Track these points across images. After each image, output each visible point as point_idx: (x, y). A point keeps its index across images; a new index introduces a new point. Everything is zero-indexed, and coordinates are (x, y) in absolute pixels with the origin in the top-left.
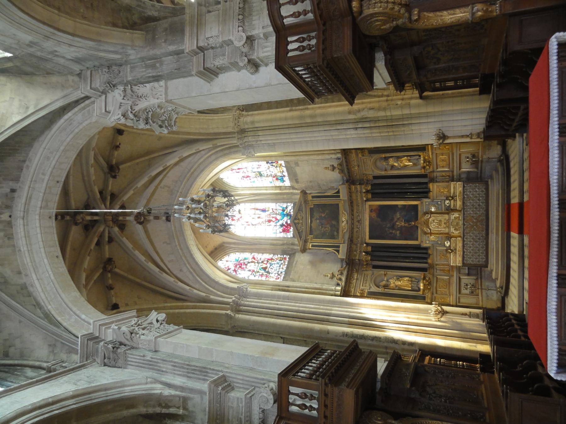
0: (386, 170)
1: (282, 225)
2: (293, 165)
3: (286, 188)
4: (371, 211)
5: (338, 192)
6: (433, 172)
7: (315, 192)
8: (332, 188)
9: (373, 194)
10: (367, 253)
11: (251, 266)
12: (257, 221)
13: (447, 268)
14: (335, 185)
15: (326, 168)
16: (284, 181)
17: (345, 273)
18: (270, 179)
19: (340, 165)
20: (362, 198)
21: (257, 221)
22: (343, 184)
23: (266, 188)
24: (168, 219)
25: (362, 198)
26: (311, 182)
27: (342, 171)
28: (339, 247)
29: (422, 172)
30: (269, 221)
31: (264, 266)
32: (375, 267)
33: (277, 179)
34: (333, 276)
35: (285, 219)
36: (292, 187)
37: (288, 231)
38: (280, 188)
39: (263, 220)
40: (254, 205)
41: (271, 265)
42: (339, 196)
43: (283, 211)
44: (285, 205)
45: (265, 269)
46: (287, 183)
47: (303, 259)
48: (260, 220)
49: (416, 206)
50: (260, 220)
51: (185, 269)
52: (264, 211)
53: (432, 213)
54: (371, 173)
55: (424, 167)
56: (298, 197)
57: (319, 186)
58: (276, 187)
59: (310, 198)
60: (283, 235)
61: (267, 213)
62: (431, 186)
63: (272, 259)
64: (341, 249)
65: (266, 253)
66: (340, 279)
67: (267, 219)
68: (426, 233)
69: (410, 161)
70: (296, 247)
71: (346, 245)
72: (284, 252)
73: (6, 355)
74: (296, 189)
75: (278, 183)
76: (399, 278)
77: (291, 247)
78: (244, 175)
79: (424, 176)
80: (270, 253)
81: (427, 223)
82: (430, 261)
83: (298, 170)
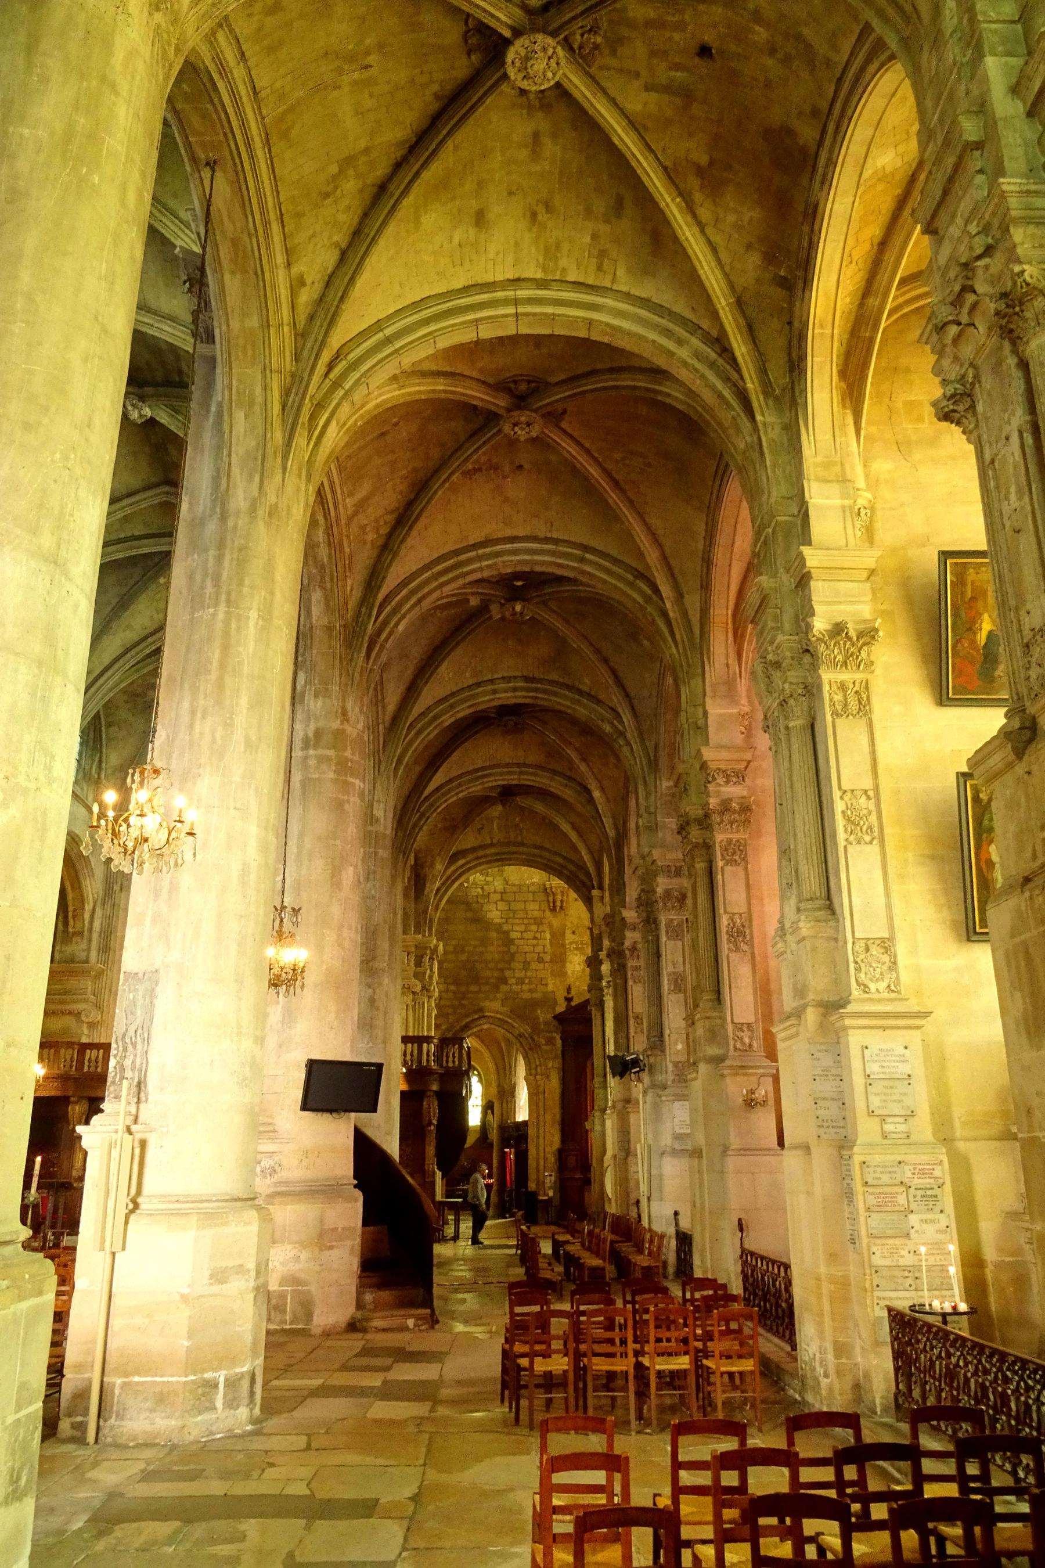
73: (109, 725)
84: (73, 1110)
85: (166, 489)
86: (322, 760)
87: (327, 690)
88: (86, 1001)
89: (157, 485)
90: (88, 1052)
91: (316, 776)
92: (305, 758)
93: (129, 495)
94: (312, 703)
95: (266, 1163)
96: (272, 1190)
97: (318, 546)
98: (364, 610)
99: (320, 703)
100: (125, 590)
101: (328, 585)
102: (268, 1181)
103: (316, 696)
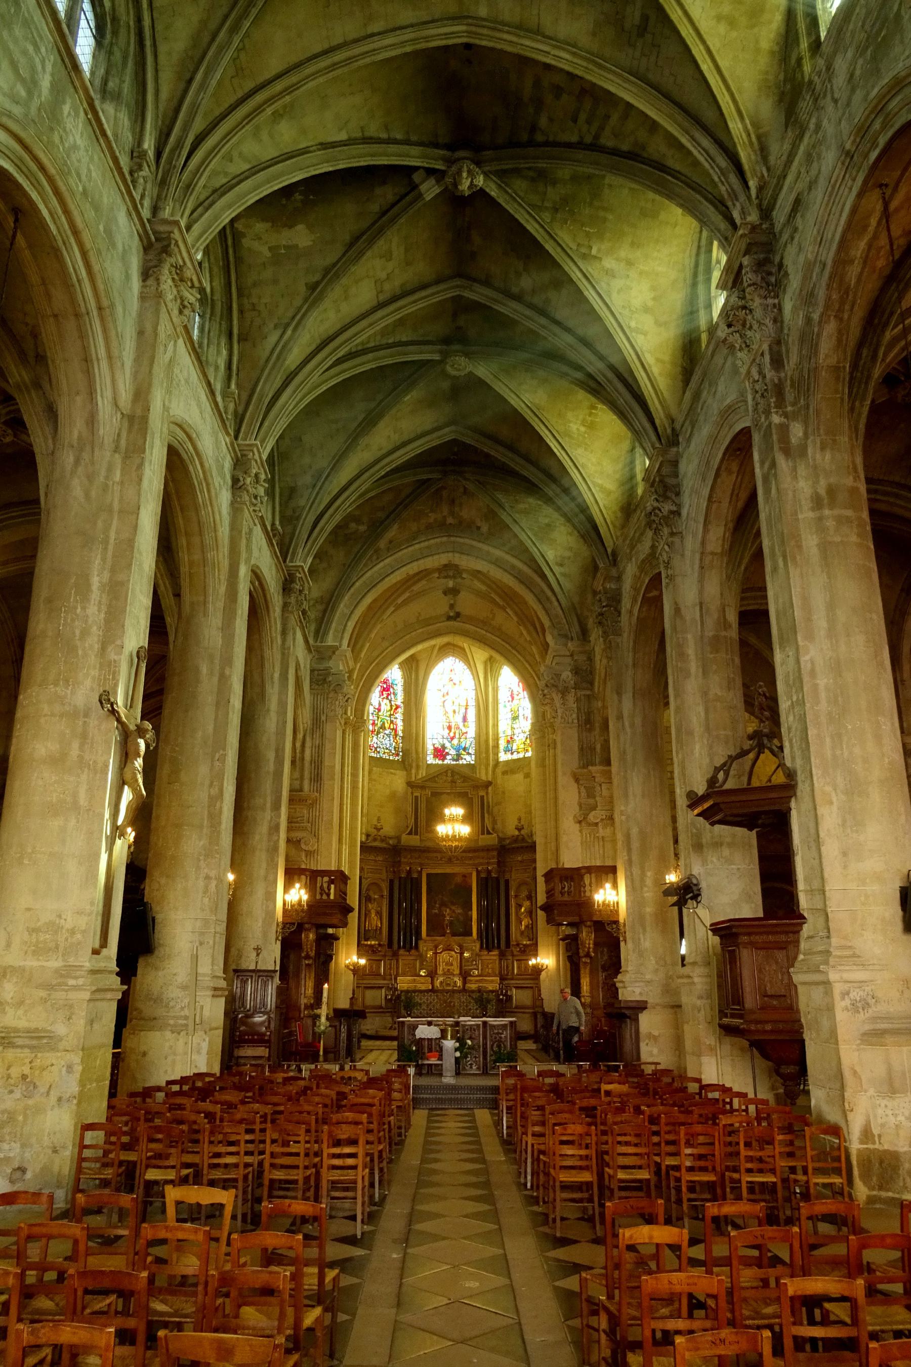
0: (516, 896)
1: (444, 747)
2: (526, 770)
3: (496, 754)
4: (464, 876)
5: (489, 833)
6: (513, 955)
7: (491, 799)
8: (494, 822)
9: (486, 879)
10: (409, 872)
11: (386, 705)
12: (450, 709)
13: (393, 972)
14: (499, 826)
15: (519, 819)
16: (505, 752)
17: (384, 845)
18: (509, 733)
19: (523, 840)
20: (481, 864)
21: (450, 709)
22: (501, 839)
23: (496, 725)
24: (449, 618)
25: (481, 864)
26: (504, 793)
27: (516, 839)
28: (416, 834)
29: (513, 943)
30: (450, 728)
31: (387, 725)
32: (391, 882)
33: (508, 742)
34: (379, 830)
35: (453, 752)
36: (497, 763)
37: (435, 756)
38: (497, 746)
39: (451, 719)
40: (472, 703)
41: (389, 736)
42: (483, 834)
43: (465, 749)
44: (472, 751)
45: (383, 727)
46: (503, 757)
47: (398, 782)
48: (451, 714)
49: (470, 934)
50: (451, 714)
51: (386, 644)
52: (465, 719)
53: (462, 954)
54: (513, 877)
55: (518, 945)
56: (484, 778)
57: (498, 804)
58: (497, 739)
59: (482, 793)
60: (430, 749)
61: (461, 725)
62: (496, 952)
63: (396, 735)
64: (414, 837)
65: (404, 726)
66: (375, 840)
67: (453, 725)
68: (436, 947)
69: (527, 927)
70: (413, 771)
71: (418, 844)
72: (406, 753)
74: (494, 772)
75: (502, 744)
76: (379, 914)
77: (414, 765)
78: (515, 693)
79: (508, 944)
80: (403, 731)
81: (449, 949)
82: (402, 952)
83: (519, 777)
84: (307, 937)
85: (458, 282)
86: (840, 520)
87: (834, 441)
88: (304, 829)
89: (451, 278)
90: (319, 879)
91: (838, 539)
92: (820, 519)
93: (424, 287)
94: (818, 456)
95: (855, 994)
96: (867, 1027)
97: (852, 262)
98: (865, 352)
99: (828, 456)
100: (372, 405)
101: (846, 316)
102: (862, 1016)
103: (823, 449)
